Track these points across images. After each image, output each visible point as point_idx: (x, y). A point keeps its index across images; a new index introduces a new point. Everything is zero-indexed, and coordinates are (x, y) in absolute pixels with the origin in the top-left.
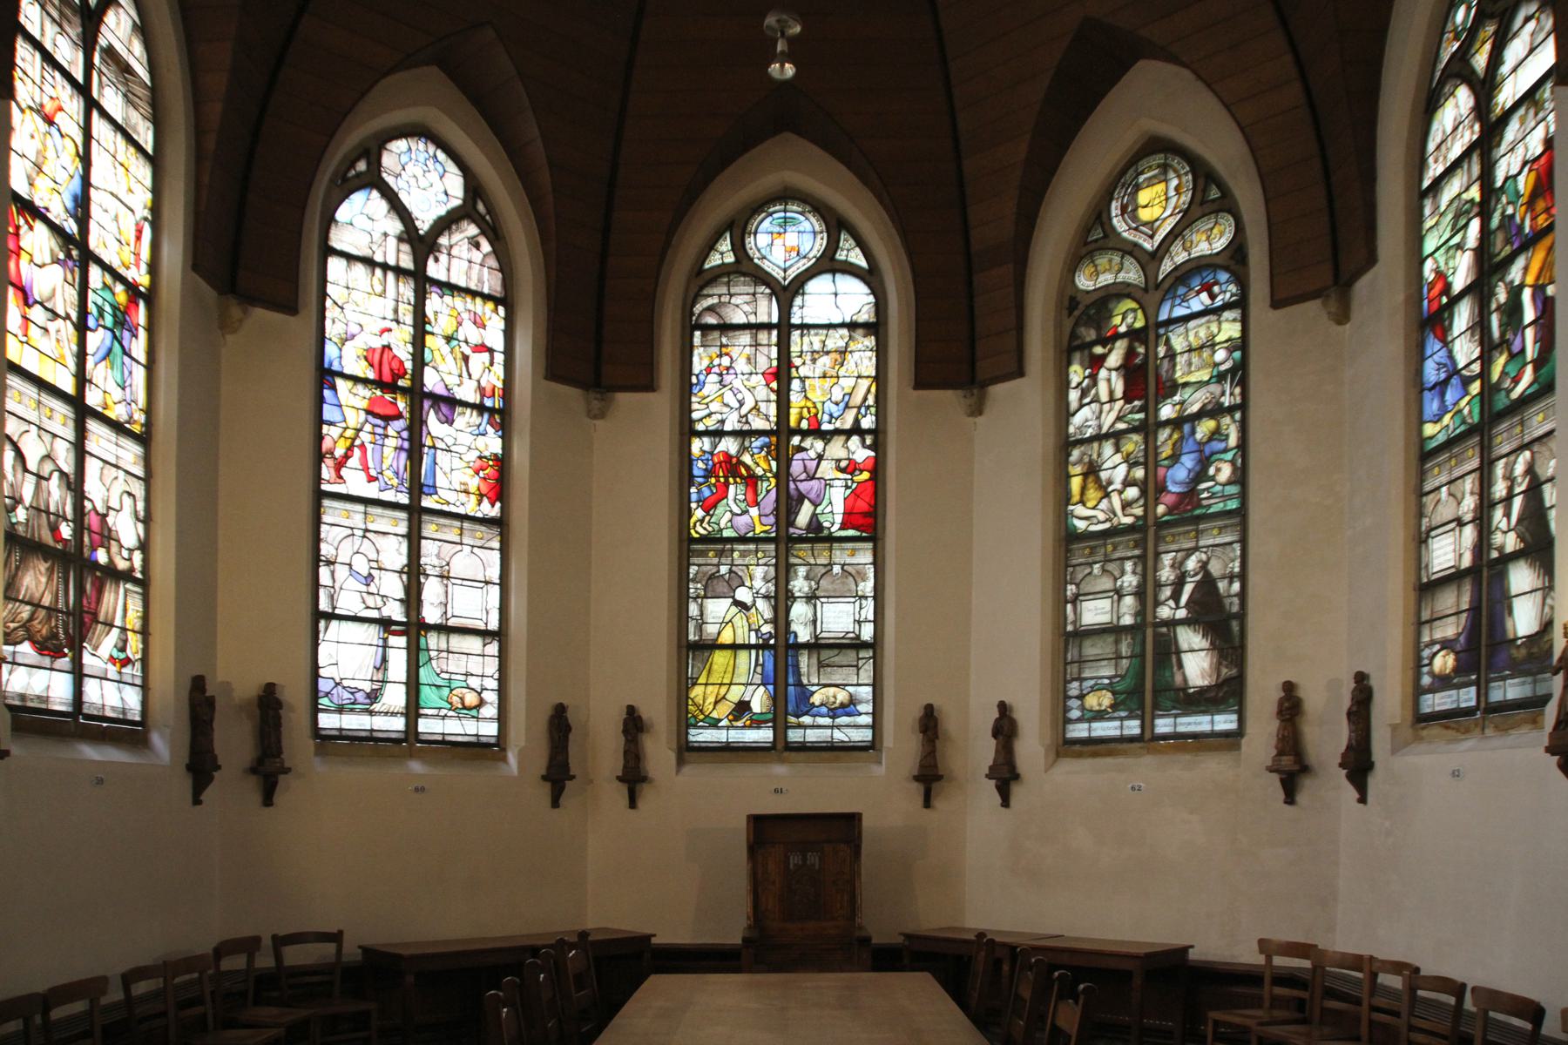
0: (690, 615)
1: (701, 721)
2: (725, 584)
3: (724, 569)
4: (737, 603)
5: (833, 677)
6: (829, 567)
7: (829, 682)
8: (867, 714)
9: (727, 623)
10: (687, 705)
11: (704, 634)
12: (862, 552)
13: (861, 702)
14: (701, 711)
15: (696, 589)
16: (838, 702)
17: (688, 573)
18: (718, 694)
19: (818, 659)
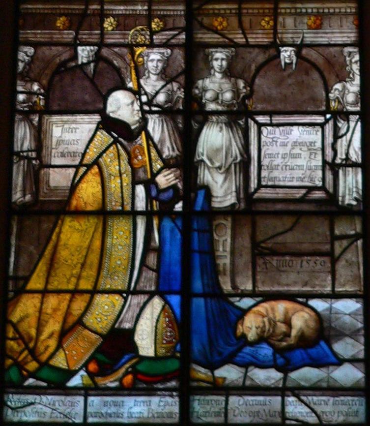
0: (17, 148)
1: (32, 375)
2: (87, 83)
3: (84, 53)
4: (109, 124)
5: (284, 278)
6: (272, 52)
7: (276, 288)
8: (353, 361)
9: (89, 167)
10: (5, 338)
11: (44, 189)
12: (335, 21)
13: (340, 334)
14: (34, 354)
15: (30, 93)
16: (294, 333)
17: (16, 61)
18: (68, 313)
19: (253, 237)
